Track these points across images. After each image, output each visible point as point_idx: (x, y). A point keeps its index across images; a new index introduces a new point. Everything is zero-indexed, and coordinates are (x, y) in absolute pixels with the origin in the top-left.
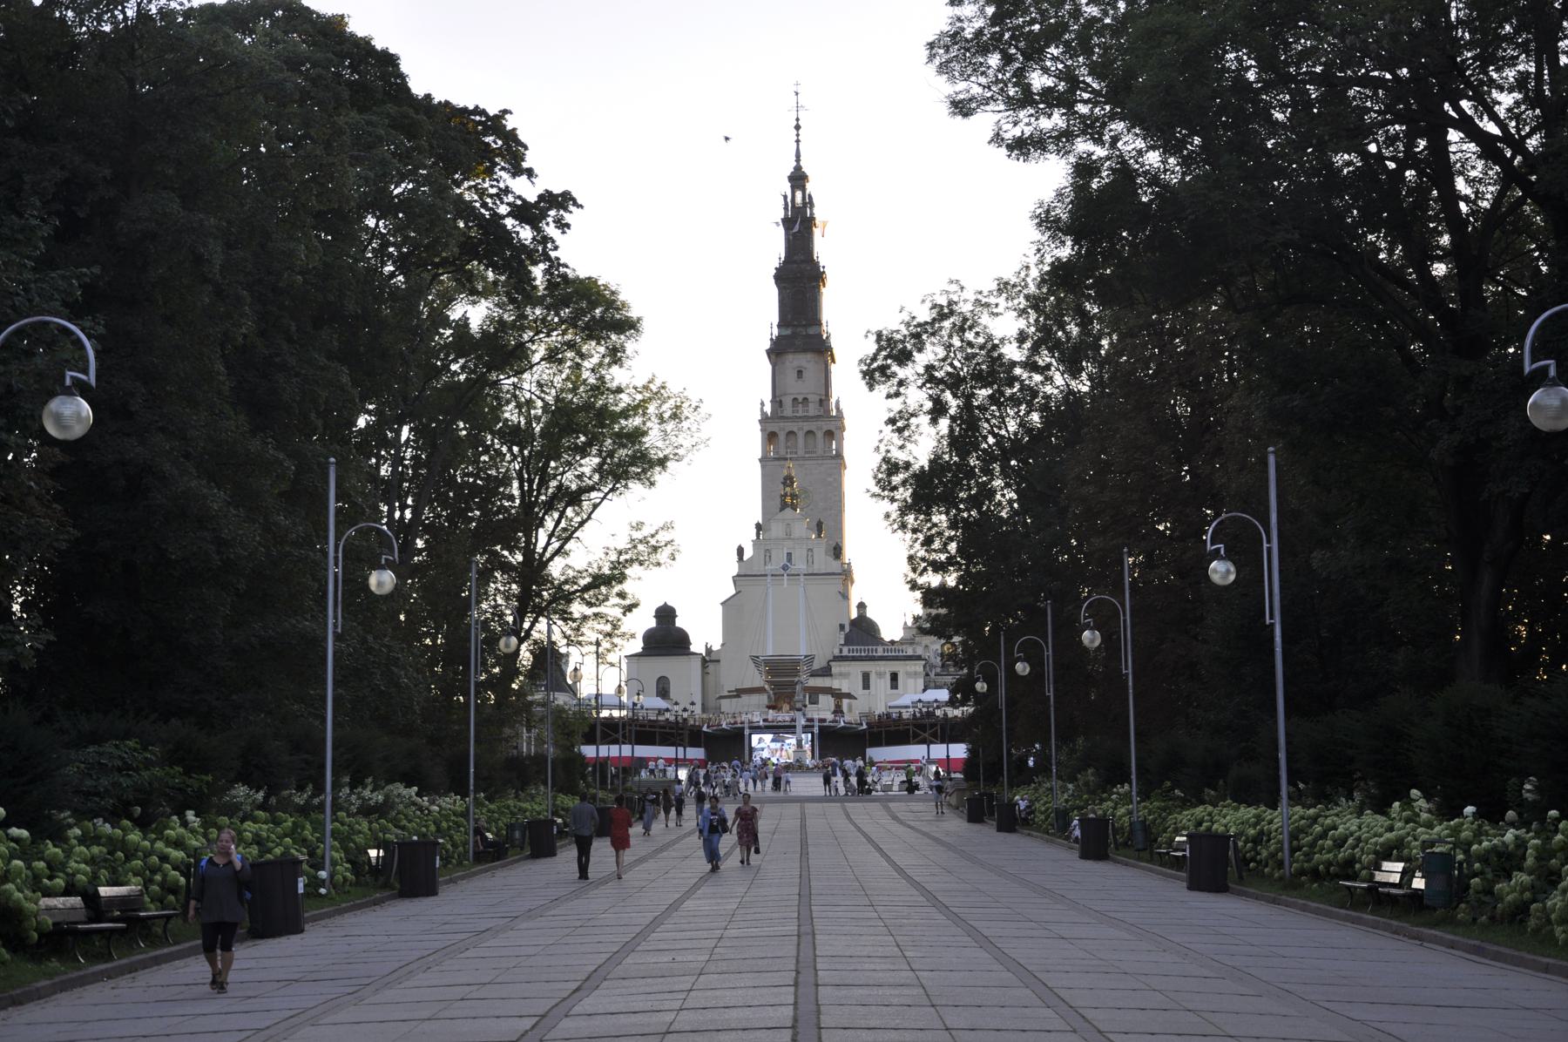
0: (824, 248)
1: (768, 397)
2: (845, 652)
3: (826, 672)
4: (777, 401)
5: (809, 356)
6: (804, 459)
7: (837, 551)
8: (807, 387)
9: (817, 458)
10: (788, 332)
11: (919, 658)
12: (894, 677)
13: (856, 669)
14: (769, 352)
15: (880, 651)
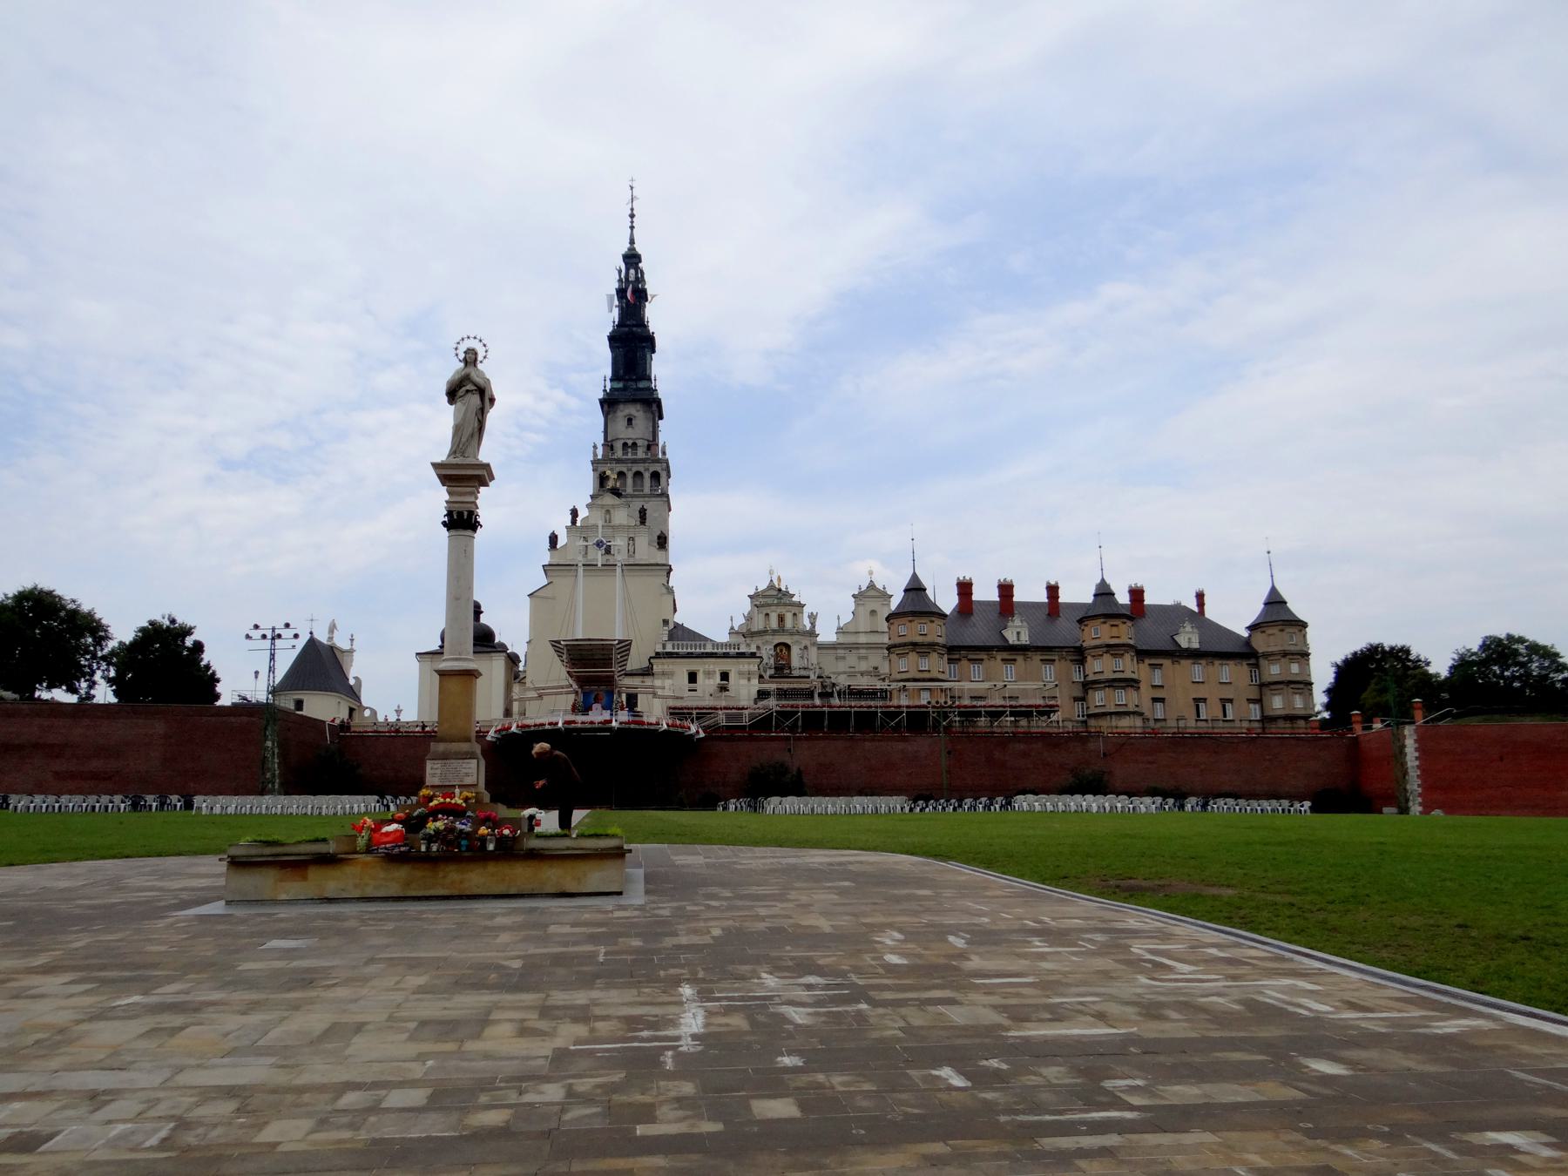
0: (656, 317)
1: (600, 441)
2: (669, 649)
3: (647, 672)
4: (609, 445)
5: (639, 406)
6: (632, 496)
7: (662, 541)
8: (639, 432)
9: (645, 496)
10: (620, 385)
11: (753, 655)
12: (725, 676)
13: (681, 669)
14: (602, 402)
15: (709, 649)
